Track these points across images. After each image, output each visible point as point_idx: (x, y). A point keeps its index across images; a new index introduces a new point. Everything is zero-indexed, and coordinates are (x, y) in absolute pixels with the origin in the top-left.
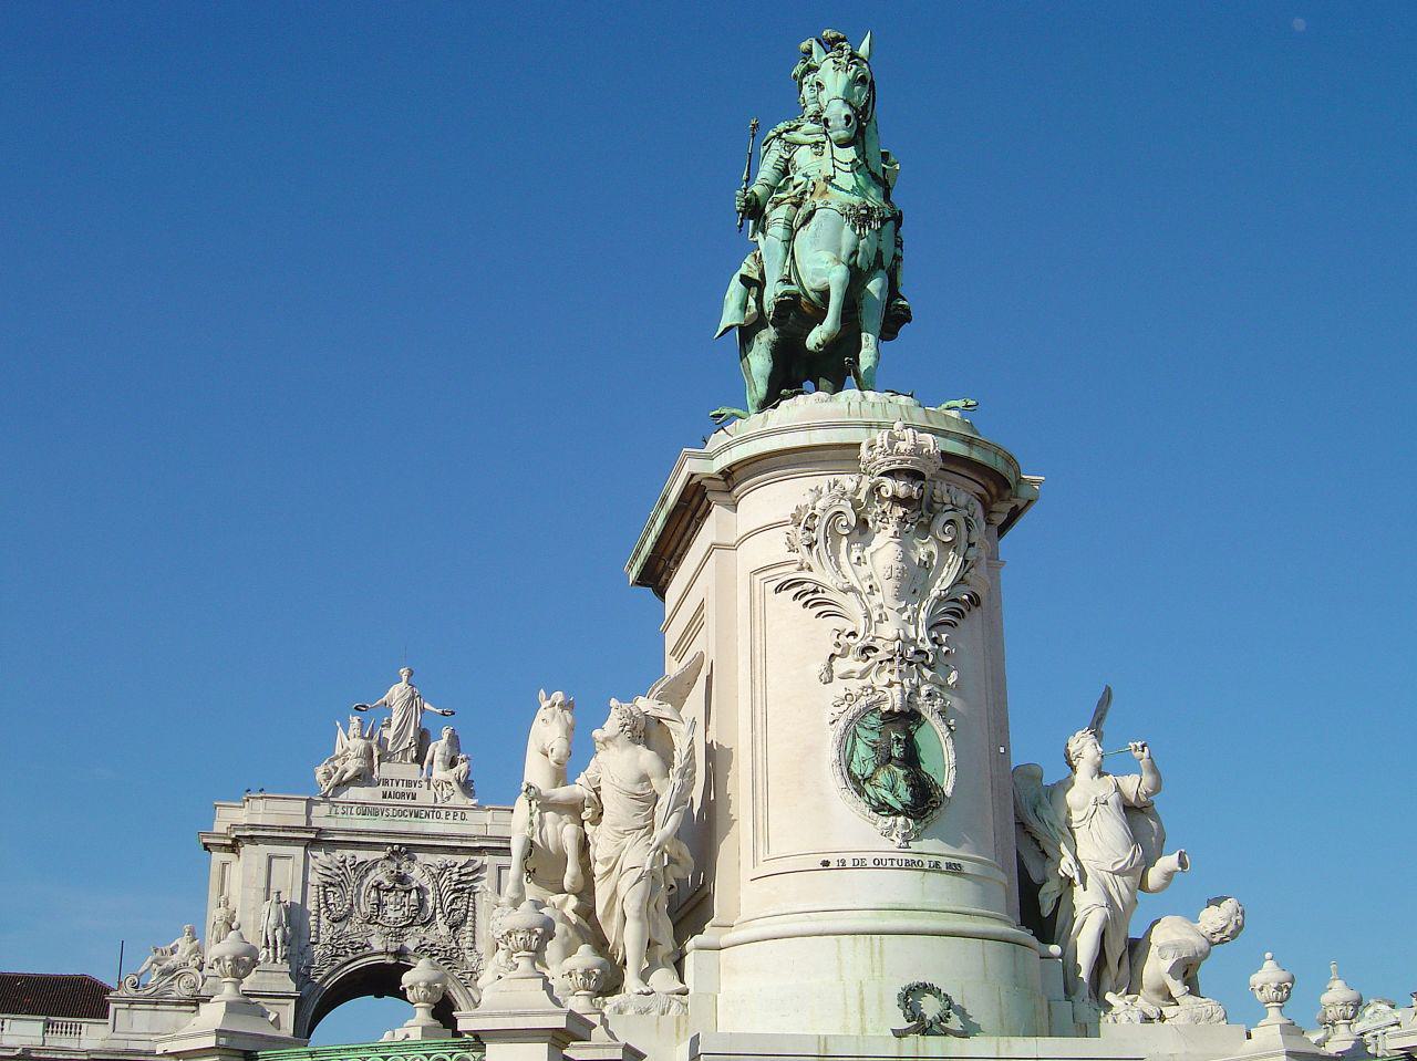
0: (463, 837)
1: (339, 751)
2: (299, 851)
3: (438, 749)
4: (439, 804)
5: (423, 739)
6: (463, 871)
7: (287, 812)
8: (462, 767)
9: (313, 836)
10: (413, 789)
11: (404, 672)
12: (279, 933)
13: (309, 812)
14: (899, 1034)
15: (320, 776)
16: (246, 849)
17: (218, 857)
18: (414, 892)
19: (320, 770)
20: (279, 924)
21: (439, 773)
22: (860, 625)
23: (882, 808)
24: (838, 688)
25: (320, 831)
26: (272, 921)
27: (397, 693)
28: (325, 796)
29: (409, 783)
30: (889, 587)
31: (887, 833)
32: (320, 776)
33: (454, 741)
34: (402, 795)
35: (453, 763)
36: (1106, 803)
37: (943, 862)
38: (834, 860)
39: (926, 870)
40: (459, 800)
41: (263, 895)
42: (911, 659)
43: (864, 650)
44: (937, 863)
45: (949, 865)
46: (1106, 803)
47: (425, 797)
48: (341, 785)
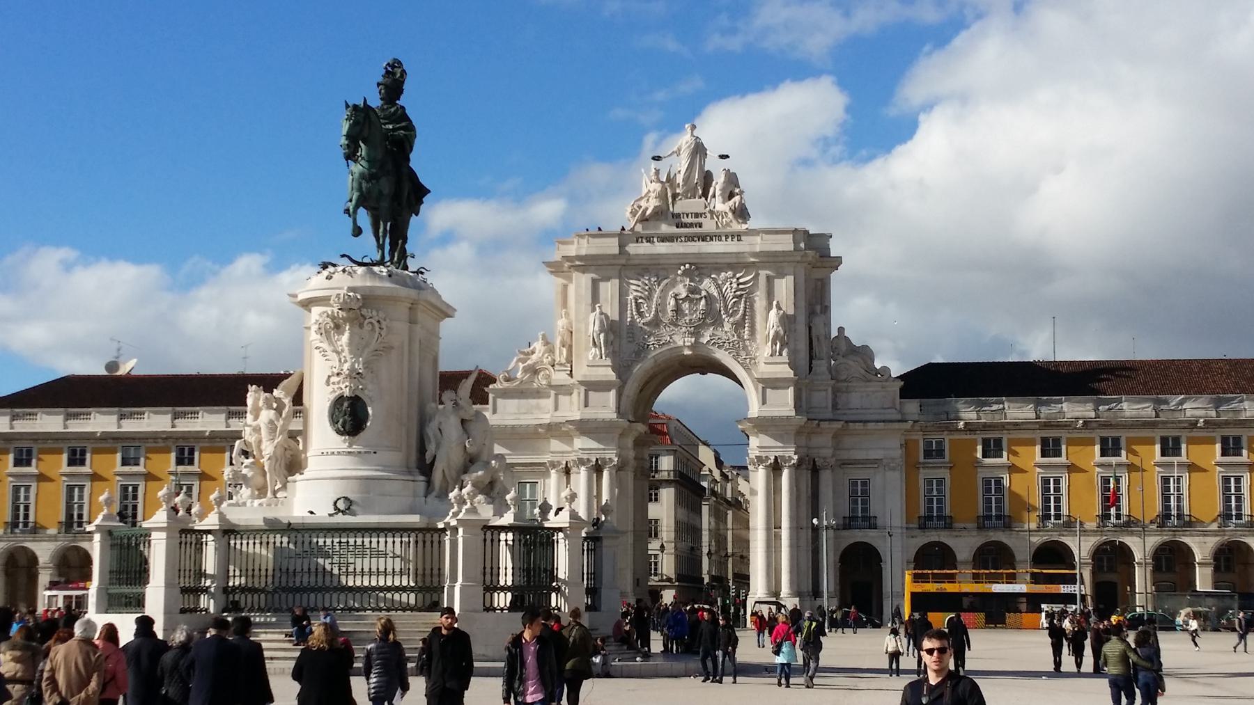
10: (700, 220)
14: (330, 515)
22: (337, 364)
23: (338, 432)
26: (597, 328)
29: (697, 215)
31: (345, 441)
33: (732, 179)
34: (691, 225)
35: (731, 196)
42: (354, 375)
47: (709, 225)
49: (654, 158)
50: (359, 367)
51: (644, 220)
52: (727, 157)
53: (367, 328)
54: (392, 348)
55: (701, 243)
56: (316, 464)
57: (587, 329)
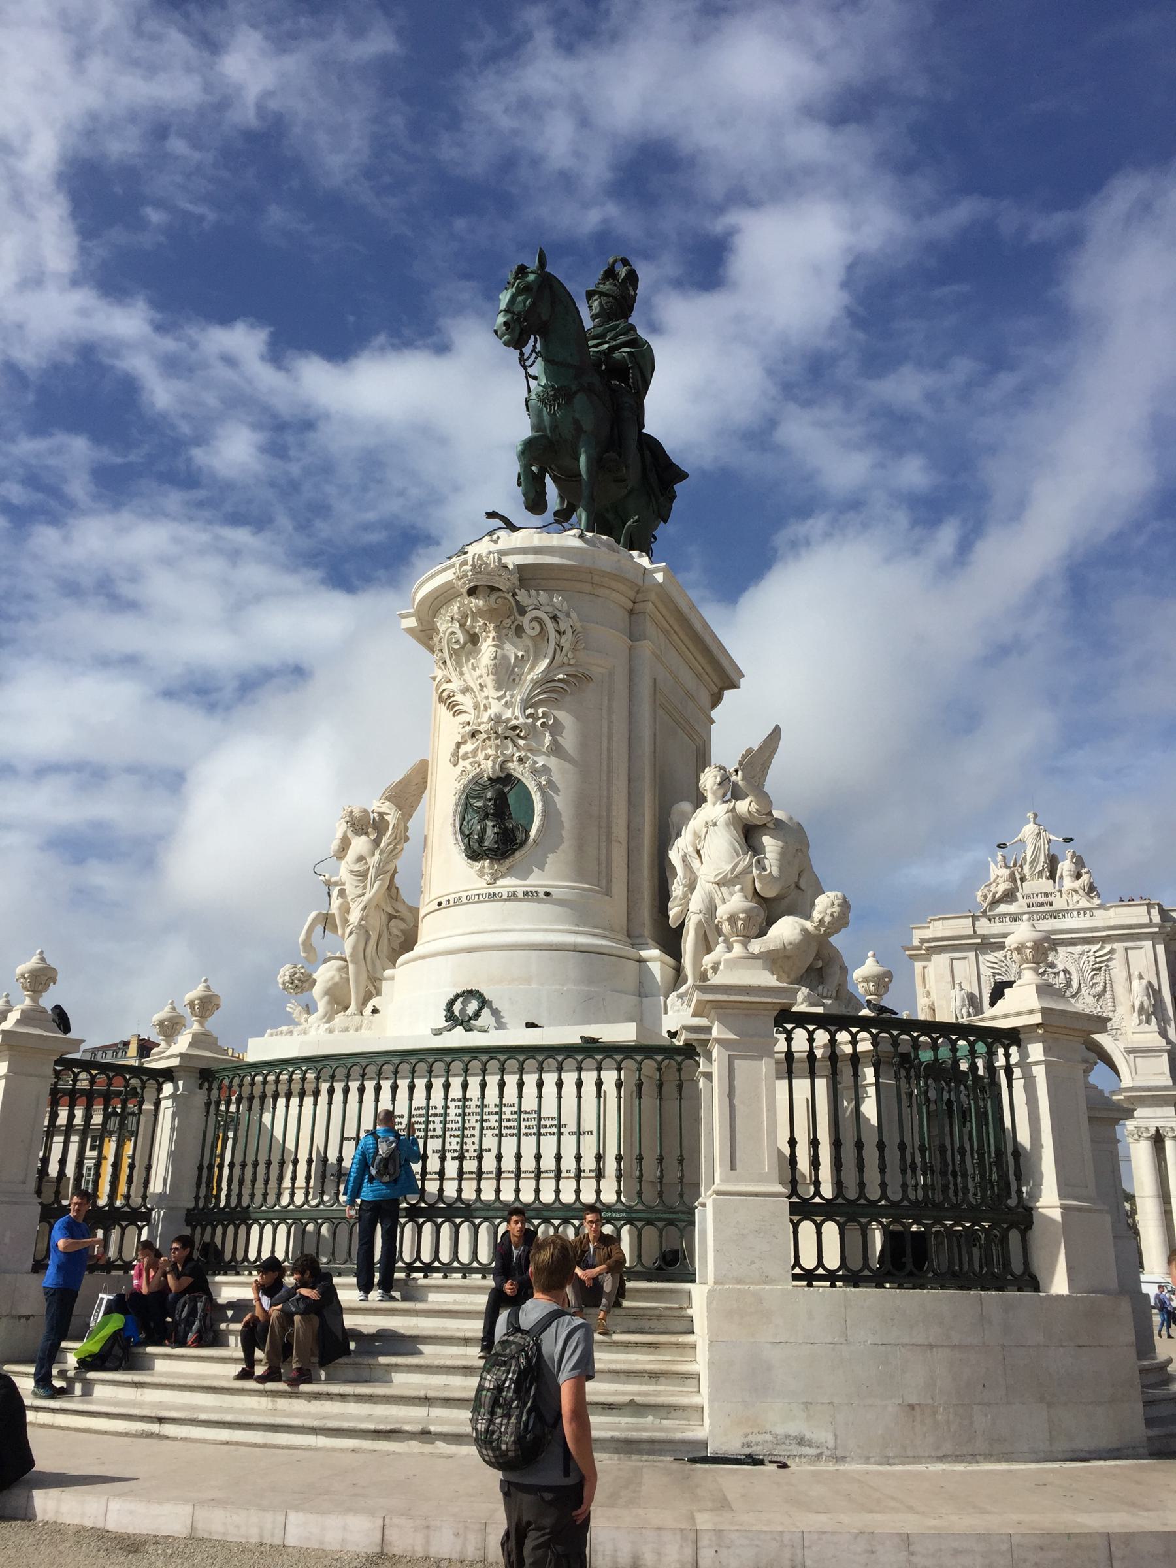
0: (1092, 930)
1: (993, 877)
2: (972, 955)
3: (1065, 867)
4: (1071, 906)
5: (1053, 863)
6: (1097, 954)
7: (962, 926)
8: (1085, 877)
9: (979, 941)
11: (1030, 815)
12: (964, 1011)
13: (974, 926)
14: (437, 1033)
15: (979, 899)
16: (935, 958)
17: (918, 965)
18: (1062, 974)
19: (979, 893)
20: (963, 1006)
21: (1068, 883)
23: (474, 855)
24: (459, 768)
25: (983, 937)
26: (958, 1003)
27: (1029, 829)
28: (984, 912)
29: (1046, 895)
30: (489, 681)
32: (979, 899)
33: (1079, 862)
35: (1078, 876)
36: (715, 824)
37: (520, 892)
38: (443, 900)
39: (506, 900)
40: (1084, 903)
41: (950, 986)
43: (473, 735)
44: (514, 894)
45: (526, 894)
46: (715, 824)
47: (1059, 903)
48: (995, 903)
49: (999, 846)
50: (514, 715)
51: (995, 903)
52: (1072, 840)
53: (531, 630)
54: (589, 679)
55: (1053, 920)
56: (434, 931)
57: (949, 1005)
